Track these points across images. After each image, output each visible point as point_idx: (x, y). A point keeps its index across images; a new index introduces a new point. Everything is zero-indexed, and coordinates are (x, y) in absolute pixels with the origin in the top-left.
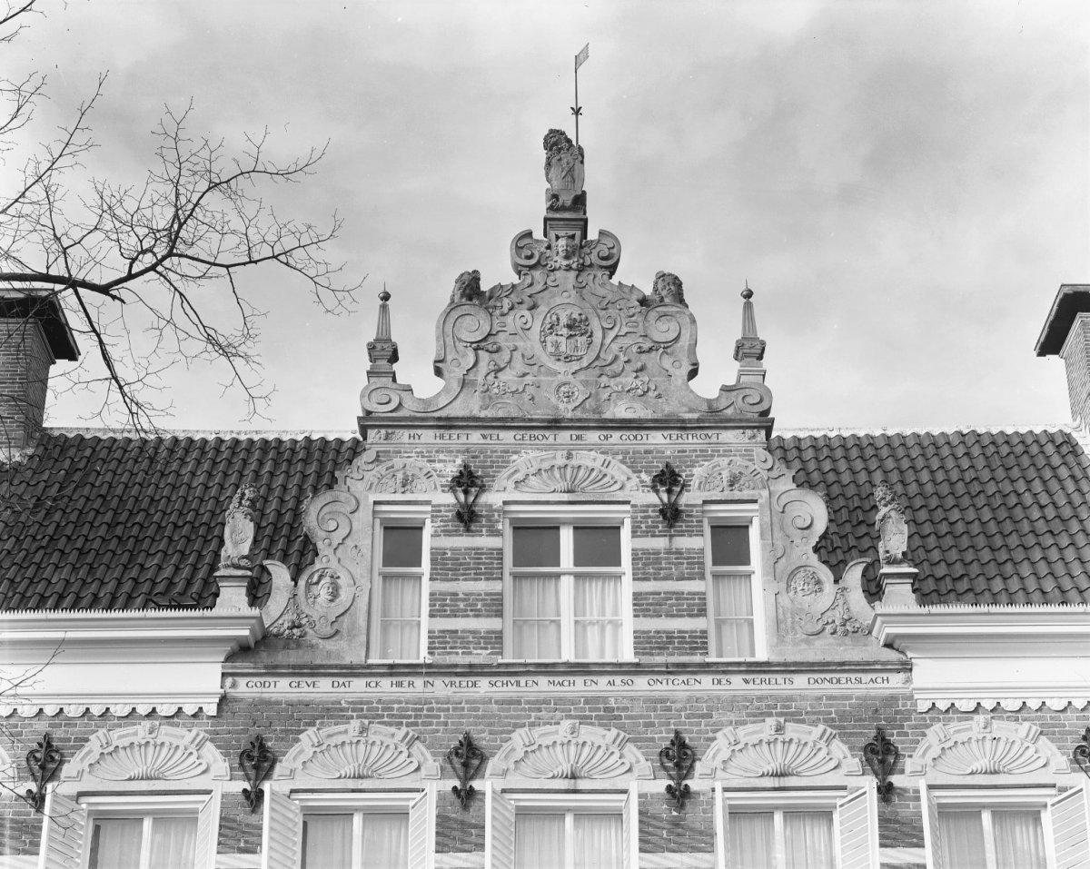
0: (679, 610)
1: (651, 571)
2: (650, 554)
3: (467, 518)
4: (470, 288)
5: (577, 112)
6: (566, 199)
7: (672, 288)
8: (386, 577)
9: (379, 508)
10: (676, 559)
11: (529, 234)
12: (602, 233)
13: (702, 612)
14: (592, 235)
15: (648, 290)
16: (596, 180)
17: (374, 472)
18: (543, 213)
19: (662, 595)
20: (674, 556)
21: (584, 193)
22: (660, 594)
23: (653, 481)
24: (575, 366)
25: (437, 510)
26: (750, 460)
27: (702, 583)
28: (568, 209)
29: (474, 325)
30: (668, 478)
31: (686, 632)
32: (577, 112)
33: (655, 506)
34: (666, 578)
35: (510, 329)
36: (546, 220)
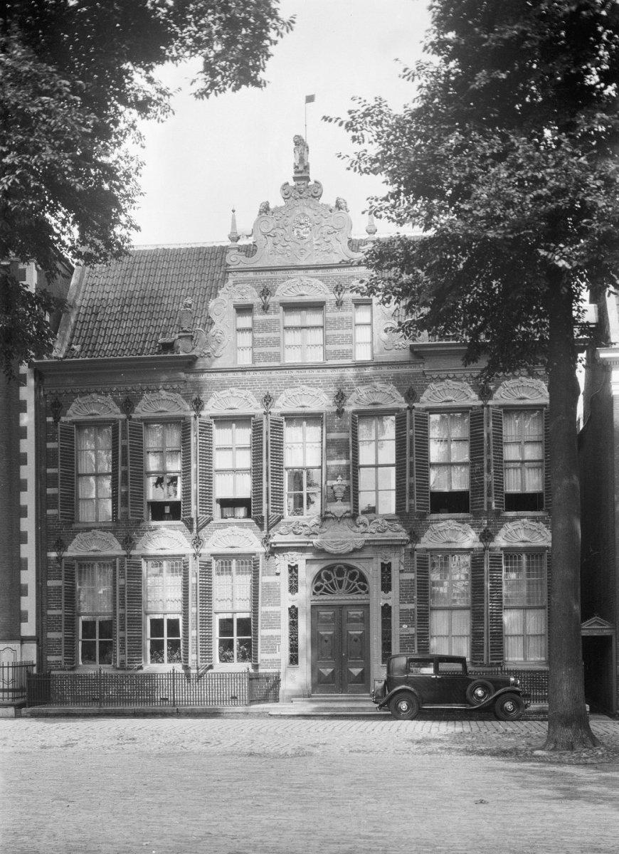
4: (265, 209)
11: (287, 184)
16: (312, 159)
18: (293, 174)
28: (302, 172)
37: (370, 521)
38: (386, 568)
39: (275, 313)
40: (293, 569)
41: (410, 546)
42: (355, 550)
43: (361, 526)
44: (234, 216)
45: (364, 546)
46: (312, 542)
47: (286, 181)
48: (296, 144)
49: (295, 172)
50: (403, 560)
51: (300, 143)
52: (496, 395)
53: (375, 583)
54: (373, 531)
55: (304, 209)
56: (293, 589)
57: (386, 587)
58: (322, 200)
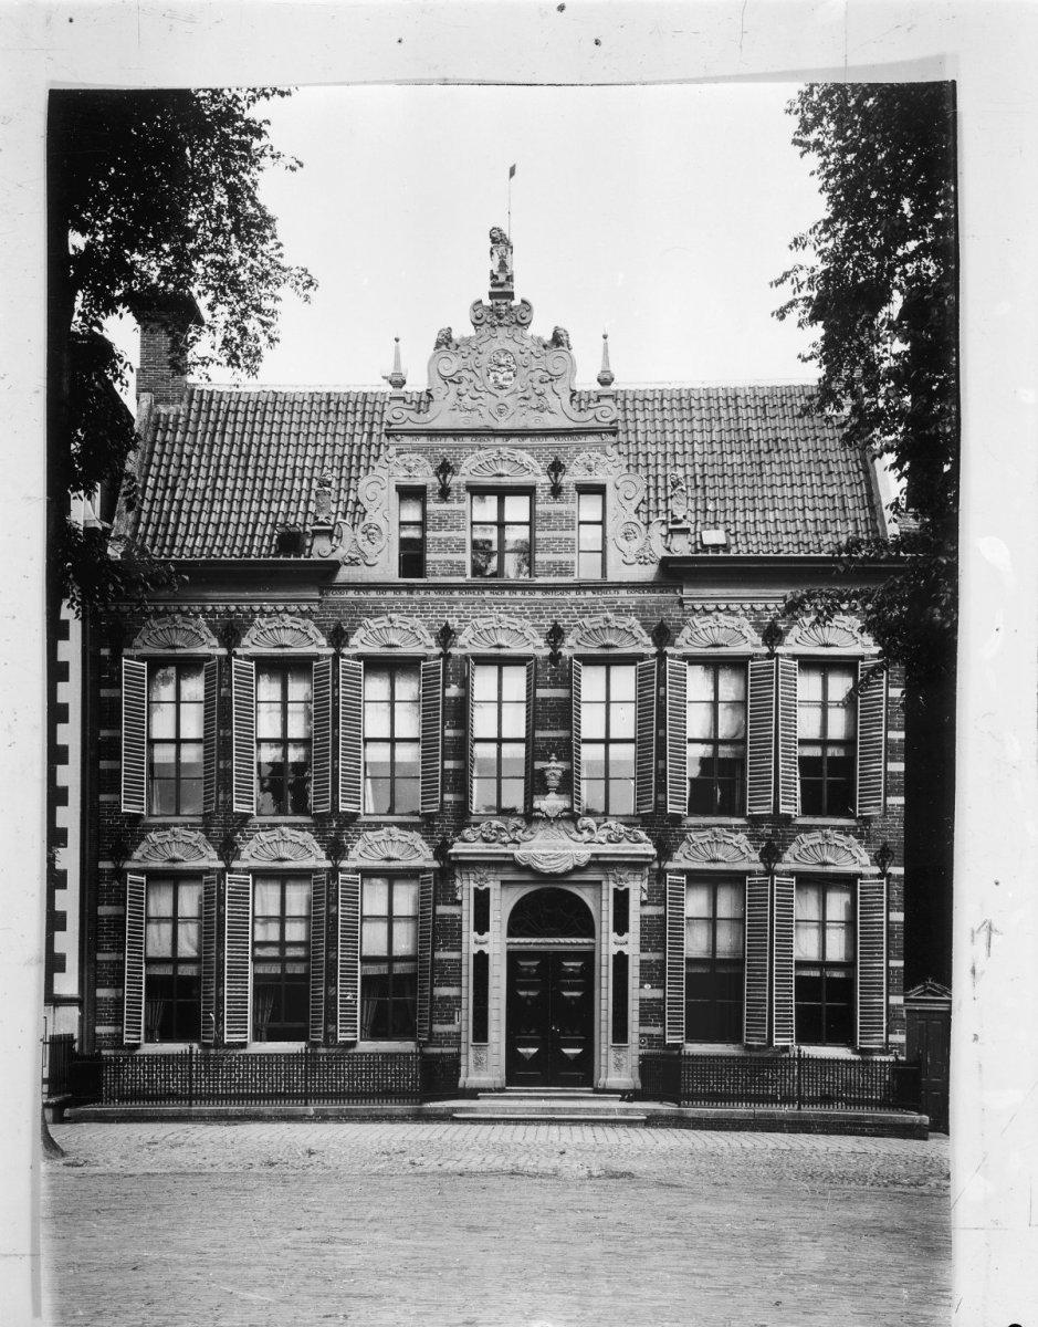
4: (445, 341)
11: (480, 302)
12: (523, 302)
16: (517, 265)
18: (490, 289)
29: (451, 366)
37: (598, 825)
38: (621, 899)
39: (461, 501)
40: (482, 899)
41: (656, 866)
42: (577, 869)
43: (585, 832)
44: (397, 348)
45: (590, 864)
46: (512, 855)
47: (477, 298)
48: (494, 240)
49: (493, 285)
50: (645, 886)
51: (499, 239)
52: (788, 639)
53: (605, 916)
54: (603, 839)
55: (502, 339)
56: (482, 925)
57: (621, 926)
58: (532, 330)
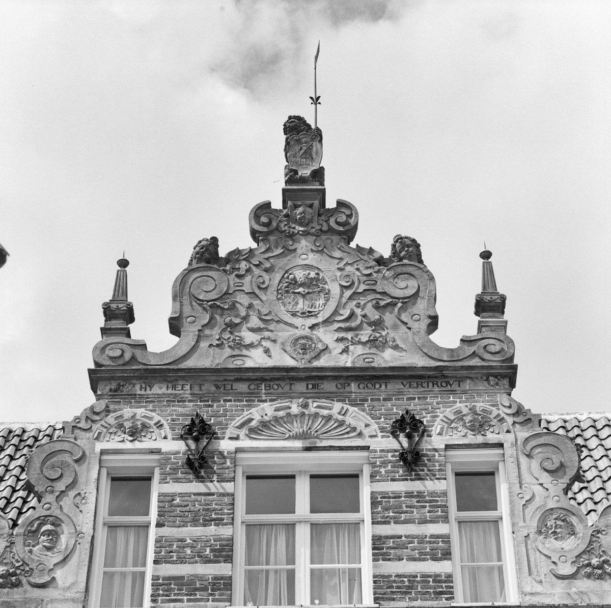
0: (421, 554)
1: (391, 514)
2: (390, 498)
3: (198, 465)
4: (207, 254)
5: (316, 100)
6: (305, 172)
7: (407, 251)
8: (112, 528)
9: (105, 457)
10: (418, 502)
11: (267, 205)
12: (341, 204)
13: (447, 555)
14: (330, 204)
15: (387, 253)
17: (103, 422)
19: (403, 538)
20: (415, 500)
21: (322, 169)
22: (400, 537)
23: (393, 427)
24: (313, 321)
25: (164, 458)
26: (493, 406)
27: (447, 525)
28: (304, 185)
29: (211, 285)
30: (408, 425)
31: (430, 576)
32: (316, 100)
33: (396, 451)
34: (406, 522)
35: (247, 288)
36: (284, 191)
55: (306, 257)
